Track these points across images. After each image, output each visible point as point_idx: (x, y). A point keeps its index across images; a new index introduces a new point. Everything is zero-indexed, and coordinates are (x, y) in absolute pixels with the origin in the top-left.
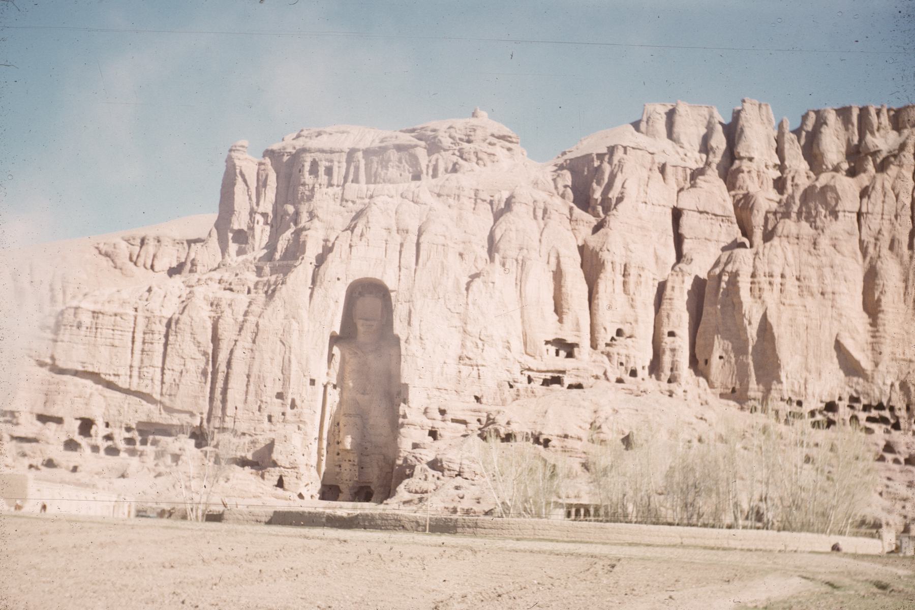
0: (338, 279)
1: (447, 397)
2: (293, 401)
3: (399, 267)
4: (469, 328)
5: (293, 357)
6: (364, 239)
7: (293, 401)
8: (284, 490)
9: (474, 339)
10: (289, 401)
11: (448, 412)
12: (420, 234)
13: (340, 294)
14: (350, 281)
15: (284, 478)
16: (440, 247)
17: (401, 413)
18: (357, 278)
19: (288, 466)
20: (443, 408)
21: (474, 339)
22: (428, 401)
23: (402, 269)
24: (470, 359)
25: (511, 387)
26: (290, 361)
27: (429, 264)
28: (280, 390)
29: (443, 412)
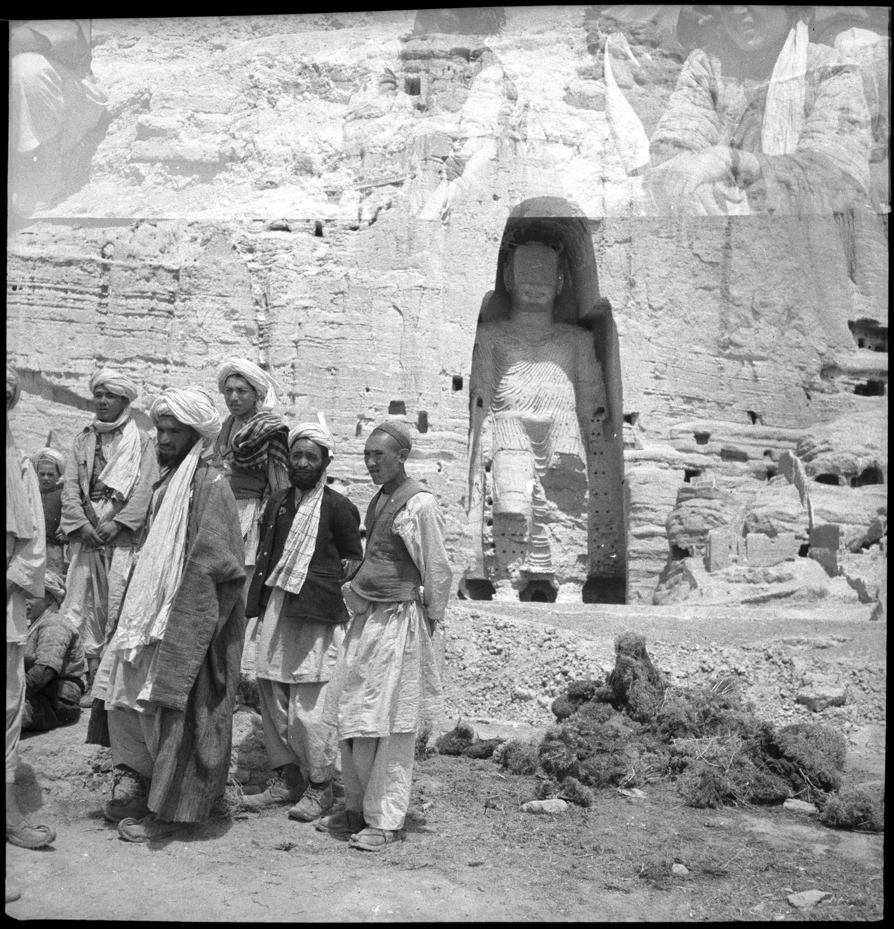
0: (495, 198)
1: (701, 412)
2: (423, 417)
4: (734, 292)
7: (423, 417)
9: (742, 311)
10: (415, 418)
13: (496, 220)
14: (518, 202)
17: (627, 439)
18: (528, 197)
20: (701, 430)
21: (742, 311)
22: (671, 420)
24: (738, 346)
25: (809, 397)
28: (397, 398)
29: (702, 438)
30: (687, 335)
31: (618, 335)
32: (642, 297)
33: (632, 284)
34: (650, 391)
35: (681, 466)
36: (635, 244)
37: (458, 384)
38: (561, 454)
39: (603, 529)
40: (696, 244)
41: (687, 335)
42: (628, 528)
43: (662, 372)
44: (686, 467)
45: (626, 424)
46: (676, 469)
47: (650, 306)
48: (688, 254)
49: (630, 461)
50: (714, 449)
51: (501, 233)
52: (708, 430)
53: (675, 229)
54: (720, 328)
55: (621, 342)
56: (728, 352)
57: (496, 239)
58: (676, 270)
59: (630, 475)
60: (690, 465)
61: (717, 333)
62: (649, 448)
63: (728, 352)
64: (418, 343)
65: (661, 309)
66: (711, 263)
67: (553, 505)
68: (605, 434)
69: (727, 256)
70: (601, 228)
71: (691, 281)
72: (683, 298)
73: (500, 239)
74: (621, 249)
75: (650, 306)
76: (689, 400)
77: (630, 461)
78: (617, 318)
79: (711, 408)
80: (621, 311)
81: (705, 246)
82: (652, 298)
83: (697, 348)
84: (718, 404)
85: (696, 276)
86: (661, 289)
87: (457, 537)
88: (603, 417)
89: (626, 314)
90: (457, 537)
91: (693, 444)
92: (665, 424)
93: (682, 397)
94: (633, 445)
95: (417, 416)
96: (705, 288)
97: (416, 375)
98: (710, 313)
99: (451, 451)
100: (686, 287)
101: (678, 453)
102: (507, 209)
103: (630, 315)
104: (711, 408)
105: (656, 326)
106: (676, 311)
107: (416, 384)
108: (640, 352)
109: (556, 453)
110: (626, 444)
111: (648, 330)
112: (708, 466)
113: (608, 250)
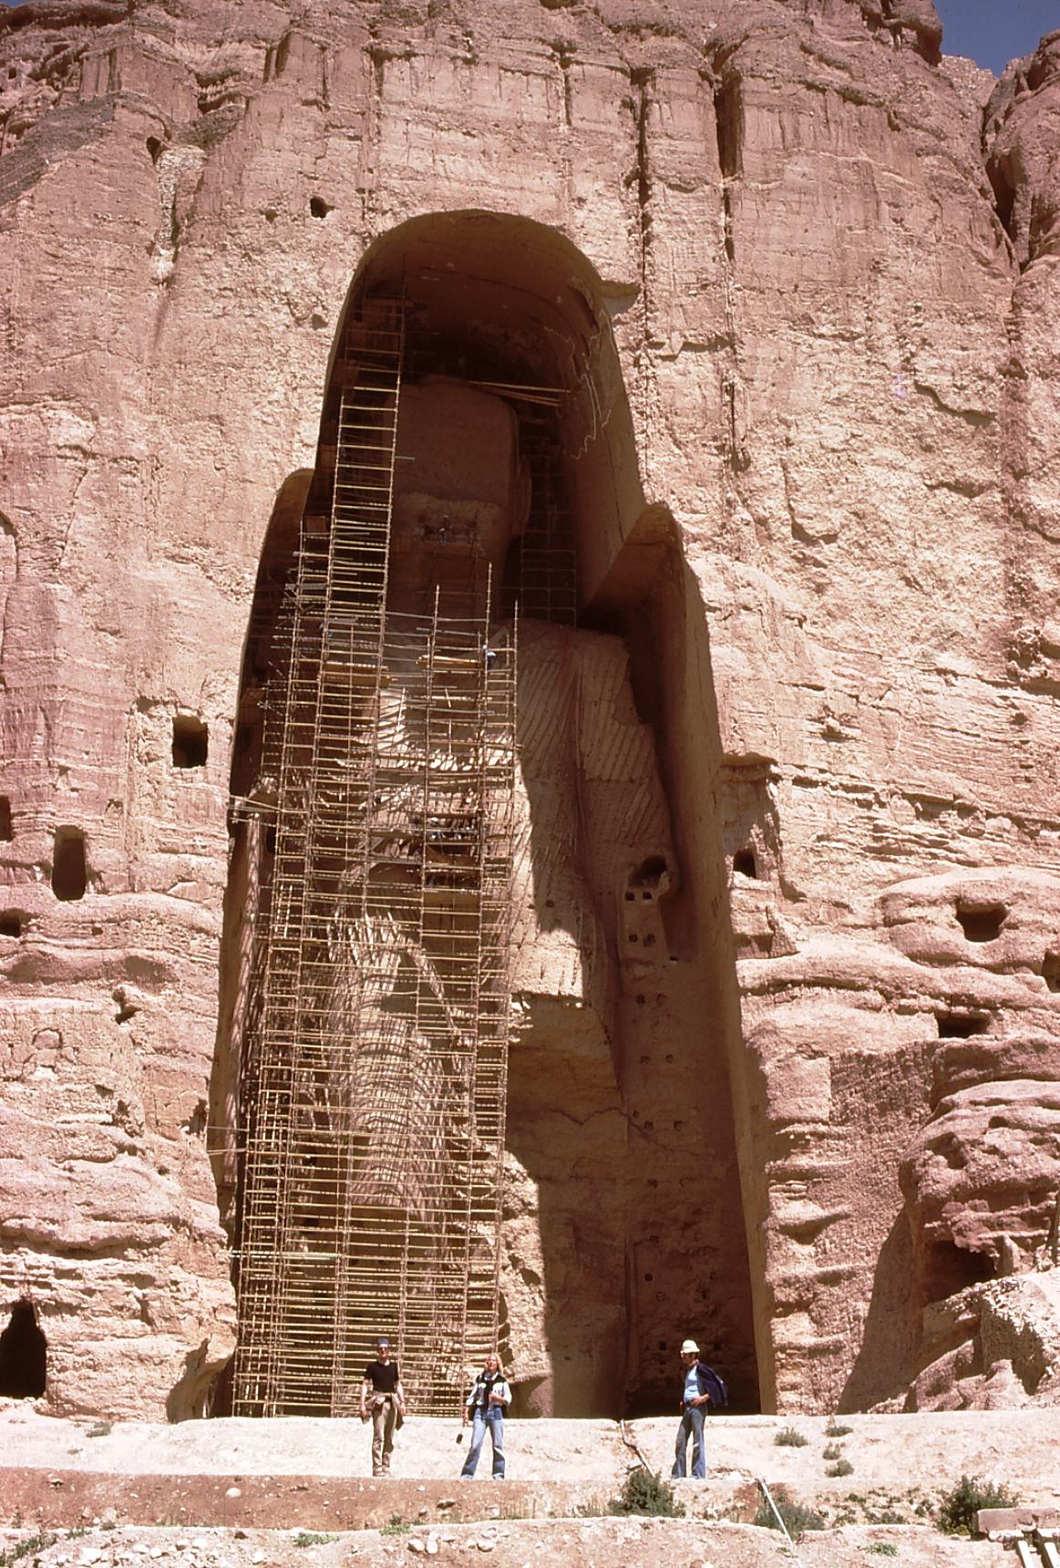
0: (319, 208)
1: (970, 847)
3: (641, 179)
5: (62, 590)
6: (444, 31)
8: (62, 1409)
11: (1016, 913)
12: (719, 52)
13: (325, 273)
14: (385, 224)
15: (47, 1324)
16: (834, 98)
17: (744, 925)
18: (422, 210)
19: (77, 1231)
20: (980, 895)
22: (881, 869)
23: (657, 188)
26: (47, 615)
27: (797, 169)
29: (982, 920)
30: (911, 617)
31: (703, 607)
32: (773, 504)
33: (739, 463)
34: (809, 774)
35: (927, 1001)
36: (743, 353)
37: (190, 746)
38: (533, 998)
39: (672, 1240)
40: (924, 361)
41: (911, 617)
42: (766, 1209)
43: (846, 720)
44: (942, 1006)
45: (739, 878)
46: (909, 1011)
47: (798, 531)
48: (901, 387)
49: (761, 991)
50: (1025, 953)
51: (334, 310)
52: (1002, 896)
53: (860, 315)
54: (1009, 603)
55: (713, 629)
56: (1034, 671)
57: (318, 322)
58: (869, 432)
59: (760, 1031)
60: (954, 999)
61: (1002, 618)
62: (817, 947)
63: (1034, 671)
64: (63, 614)
65: (830, 538)
66: (970, 416)
67: (514, 1165)
68: (669, 935)
69: (1015, 397)
70: (638, 306)
71: (916, 464)
72: (893, 511)
73: (333, 320)
74: (701, 367)
75: (798, 531)
76: (929, 807)
77: (761, 991)
78: (700, 562)
79: (999, 834)
80: (712, 545)
81: (949, 364)
82: (803, 507)
83: (944, 660)
84: (1018, 822)
85: (928, 449)
86: (828, 483)
87: (164, 1231)
88: (665, 882)
89: (728, 549)
90: (164, 1231)
91: (955, 938)
92: (860, 882)
93: (912, 799)
94: (766, 944)
95: (50, 842)
96: (957, 487)
97: (50, 711)
98: (977, 560)
99: (162, 956)
100: (906, 480)
101: (907, 962)
102: (353, 240)
103: (738, 553)
104: (999, 834)
105: (820, 589)
106: (877, 548)
107: (50, 743)
108: (773, 657)
109: (518, 996)
110: (744, 940)
111: (792, 596)
112: (1006, 1004)
113: (664, 371)
